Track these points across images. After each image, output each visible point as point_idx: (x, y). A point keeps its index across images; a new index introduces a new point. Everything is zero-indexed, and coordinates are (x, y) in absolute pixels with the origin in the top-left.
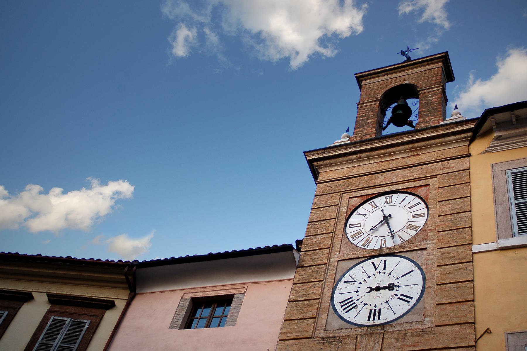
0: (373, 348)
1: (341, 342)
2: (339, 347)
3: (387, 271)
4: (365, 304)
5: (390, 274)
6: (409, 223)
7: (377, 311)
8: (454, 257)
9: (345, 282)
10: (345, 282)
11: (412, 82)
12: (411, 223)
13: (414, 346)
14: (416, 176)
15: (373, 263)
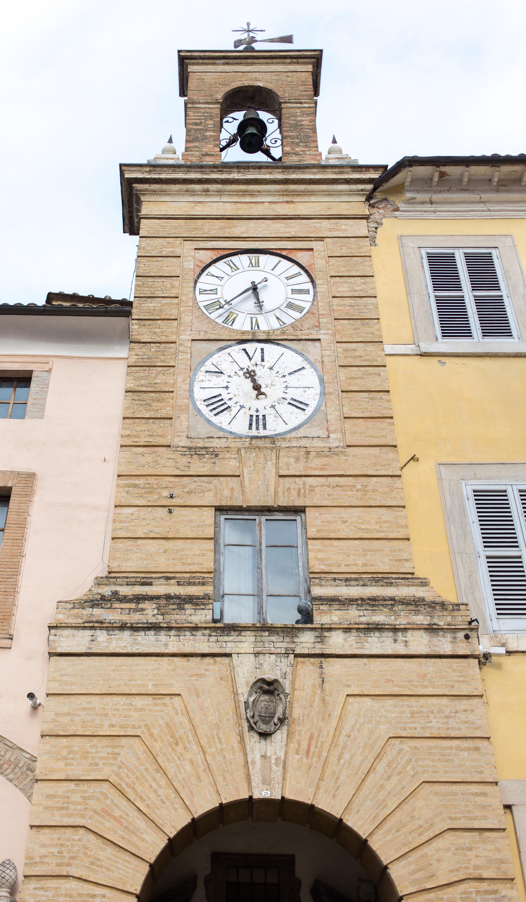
0: (264, 468)
1: (217, 455)
2: (215, 463)
3: (267, 364)
4: (242, 407)
5: (271, 369)
6: (289, 300)
7: (261, 417)
8: (361, 357)
9: (207, 372)
10: (207, 372)
11: (269, 86)
12: (292, 301)
13: (321, 469)
14: (293, 233)
15: (244, 350)
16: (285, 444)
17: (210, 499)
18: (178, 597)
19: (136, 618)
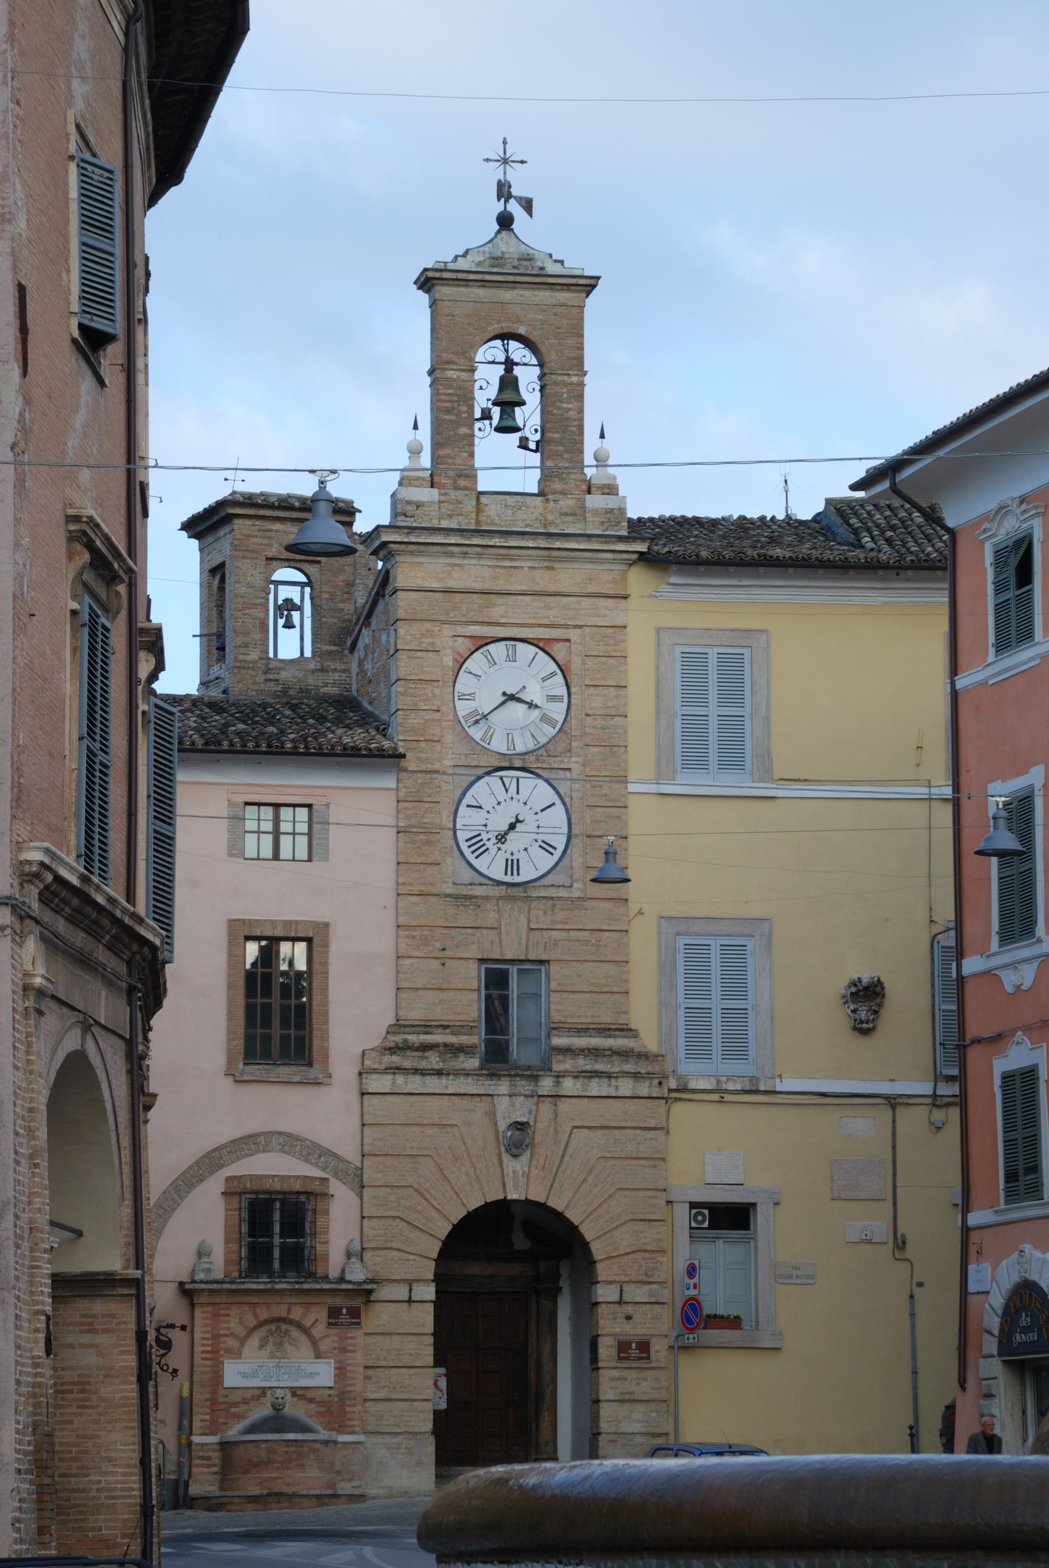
3: (523, 797)
7: (515, 862)
13: (564, 923)
16: (535, 894)
17: (473, 952)
18: (452, 1045)
19: (424, 1064)
